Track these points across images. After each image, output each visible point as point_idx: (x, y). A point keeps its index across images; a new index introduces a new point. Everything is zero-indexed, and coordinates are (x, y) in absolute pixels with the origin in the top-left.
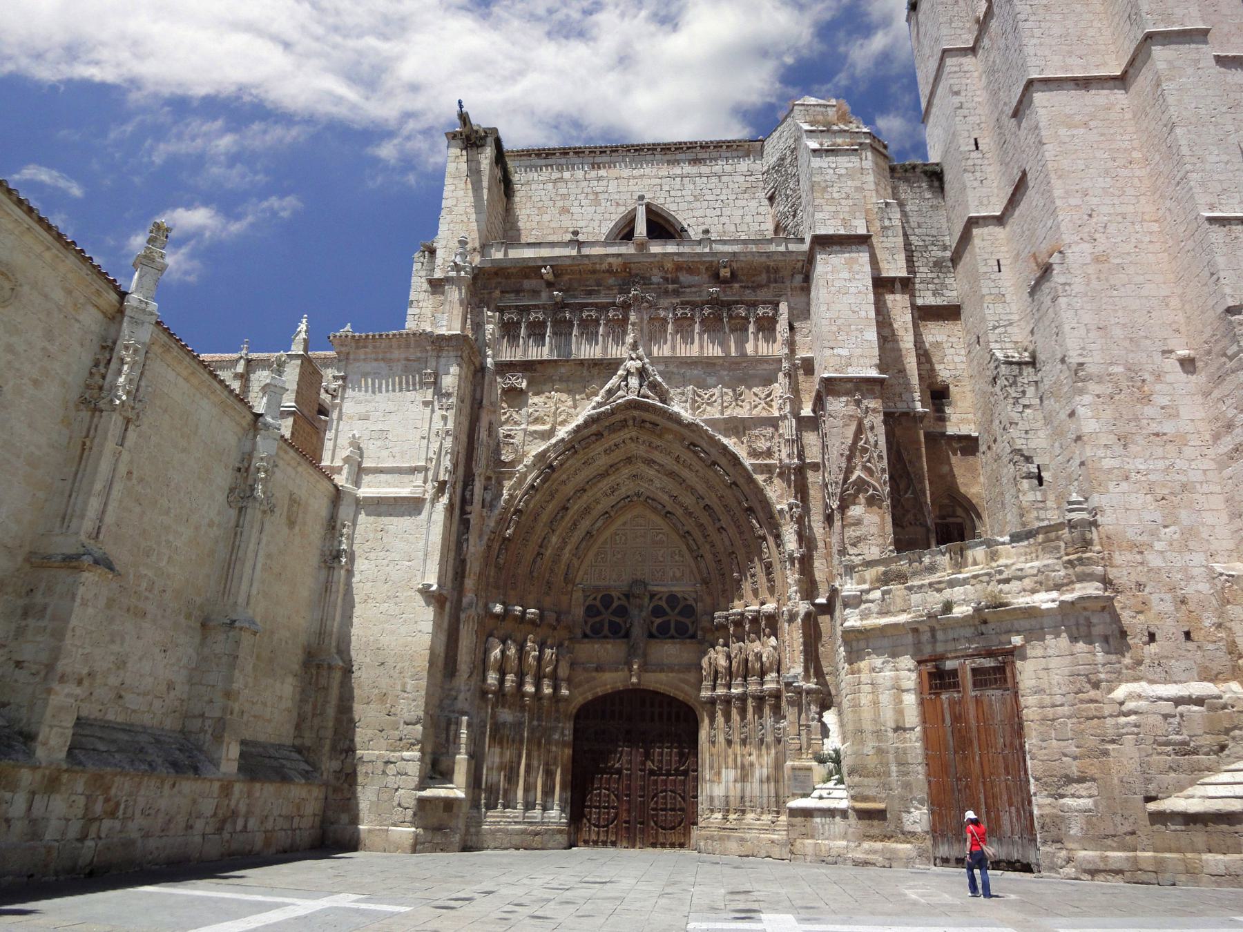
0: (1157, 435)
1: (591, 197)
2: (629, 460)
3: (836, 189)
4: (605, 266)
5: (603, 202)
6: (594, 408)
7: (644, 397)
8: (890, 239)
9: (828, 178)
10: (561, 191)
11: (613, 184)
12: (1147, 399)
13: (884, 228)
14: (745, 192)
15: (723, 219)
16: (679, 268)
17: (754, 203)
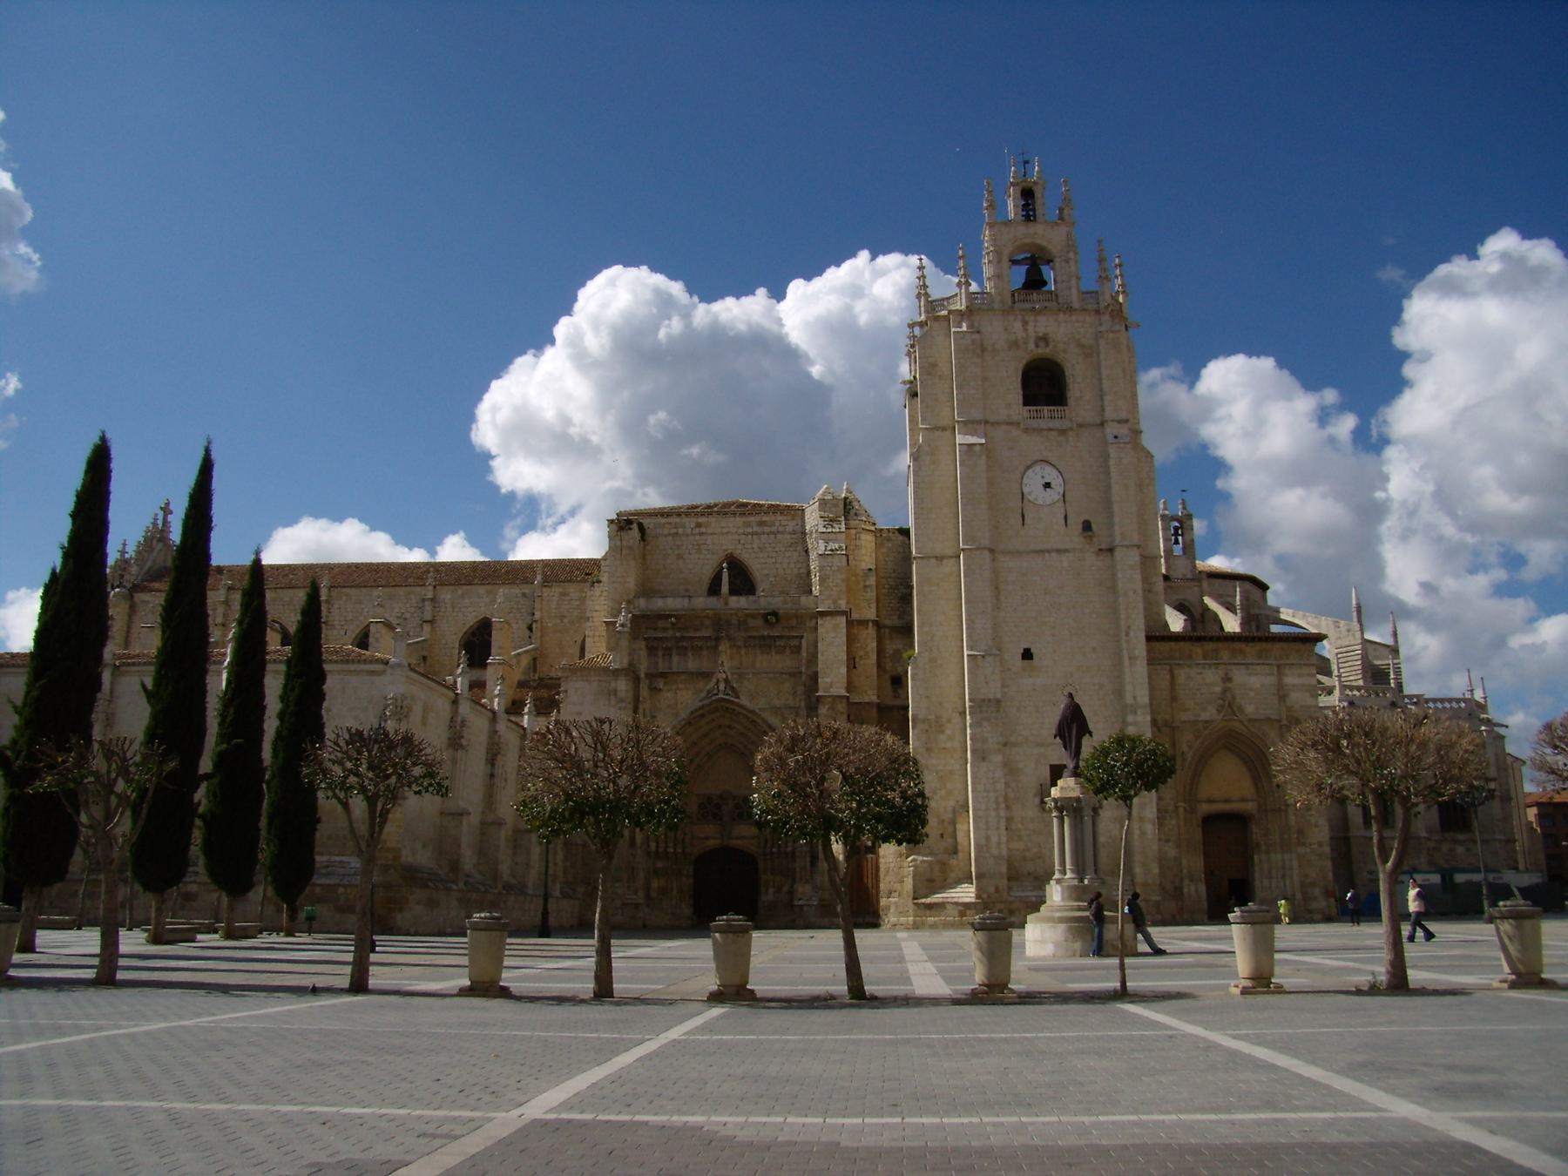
0: (944, 749)
1: (696, 547)
2: (720, 727)
3: (831, 580)
4: (704, 614)
6: (701, 701)
7: (727, 694)
8: (869, 594)
9: (827, 573)
10: (679, 543)
11: (710, 538)
12: (942, 732)
13: (865, 586)
14: (790, 546)
15: (778, 565)
16: (747, 615)
17: (796, 554)
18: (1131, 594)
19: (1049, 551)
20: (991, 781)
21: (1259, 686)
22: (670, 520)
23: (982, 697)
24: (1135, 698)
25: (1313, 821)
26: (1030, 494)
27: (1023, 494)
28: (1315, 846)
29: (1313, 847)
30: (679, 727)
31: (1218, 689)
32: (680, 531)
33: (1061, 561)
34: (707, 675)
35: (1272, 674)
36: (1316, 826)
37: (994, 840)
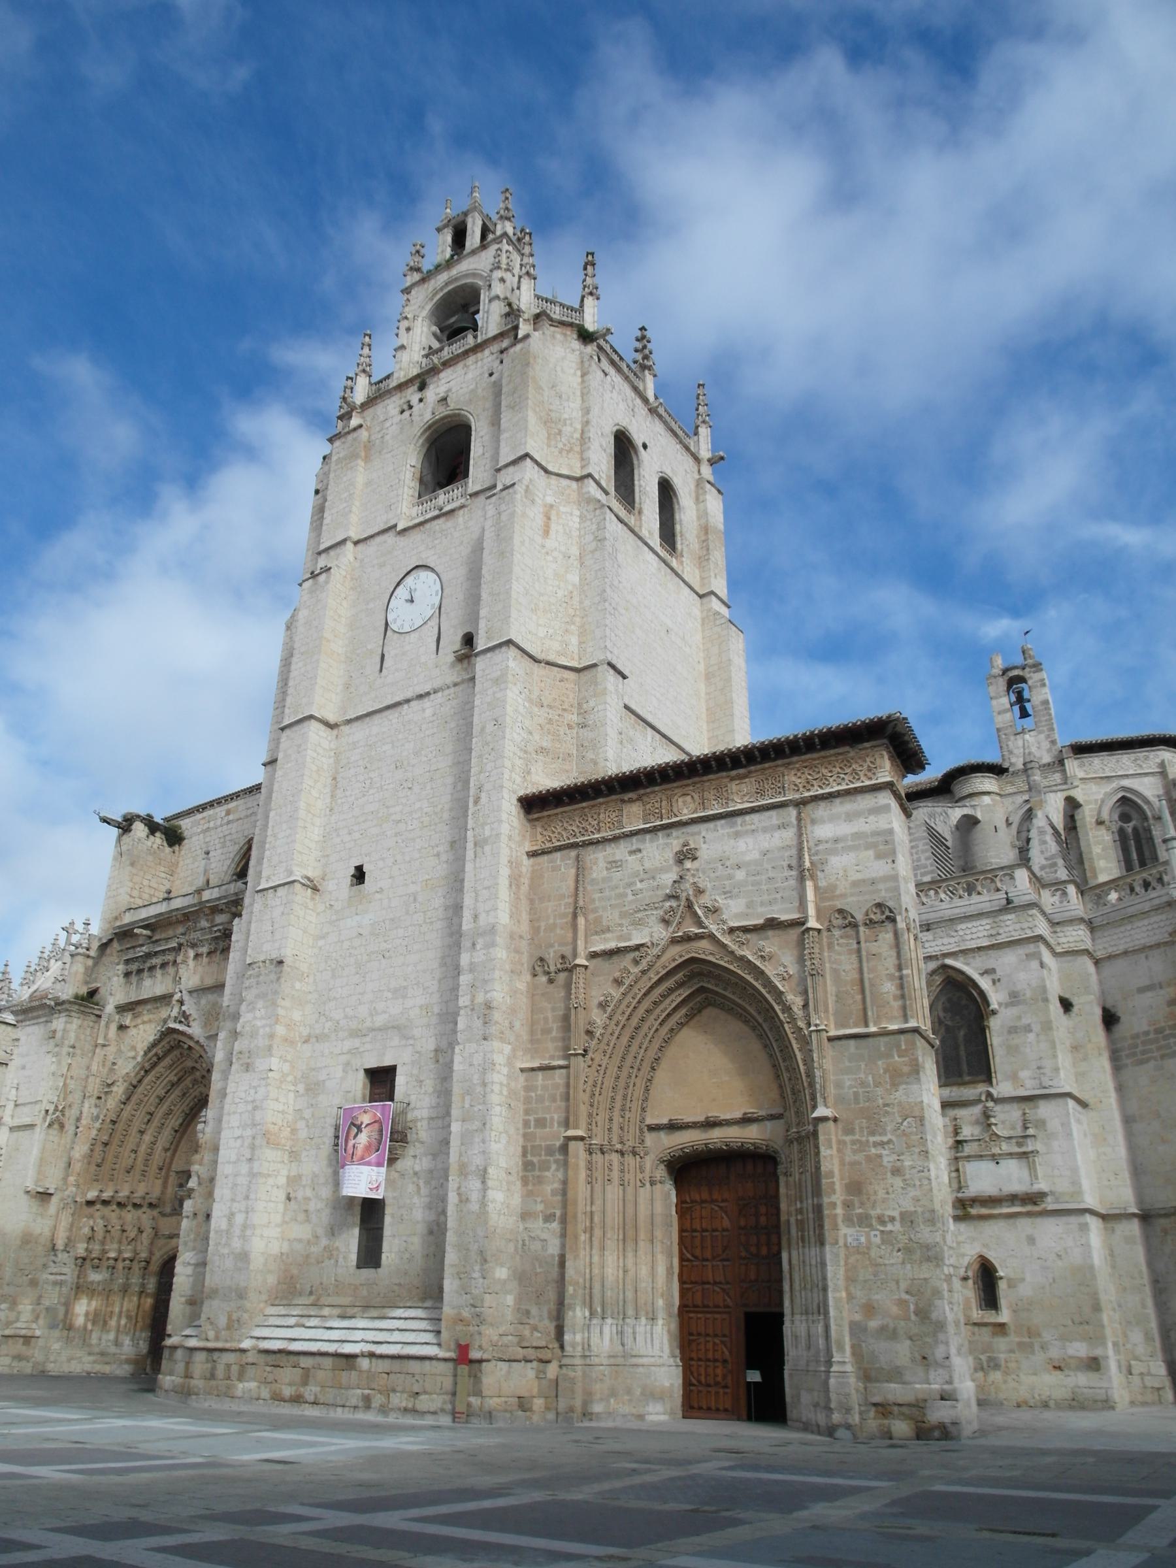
5: (228, 844)
18: (490, 728)
19: (408, 701)
20: (250, 1107)
21: (755, 855)
22: (205, 814)
23: (262, 959)
24: (476, 917)
25: (888, 1159)
26: (395, 620)
27: (387, 624)
28: (896, 1227)
29: (889, 1227)
30: (133, 1075)
31: (669, 878)
32: (212, 824)
33: (424, 710)
34: (165, 999)
35: (783, 826)
36: (897, 1171)
37: (239, 1219)
